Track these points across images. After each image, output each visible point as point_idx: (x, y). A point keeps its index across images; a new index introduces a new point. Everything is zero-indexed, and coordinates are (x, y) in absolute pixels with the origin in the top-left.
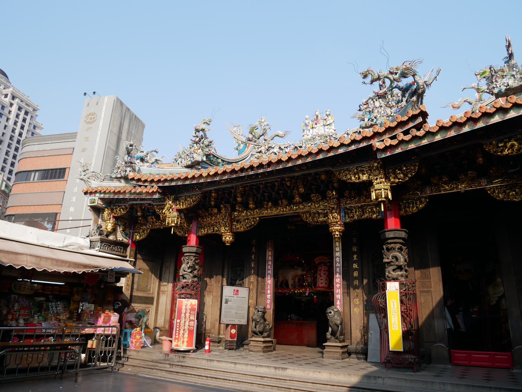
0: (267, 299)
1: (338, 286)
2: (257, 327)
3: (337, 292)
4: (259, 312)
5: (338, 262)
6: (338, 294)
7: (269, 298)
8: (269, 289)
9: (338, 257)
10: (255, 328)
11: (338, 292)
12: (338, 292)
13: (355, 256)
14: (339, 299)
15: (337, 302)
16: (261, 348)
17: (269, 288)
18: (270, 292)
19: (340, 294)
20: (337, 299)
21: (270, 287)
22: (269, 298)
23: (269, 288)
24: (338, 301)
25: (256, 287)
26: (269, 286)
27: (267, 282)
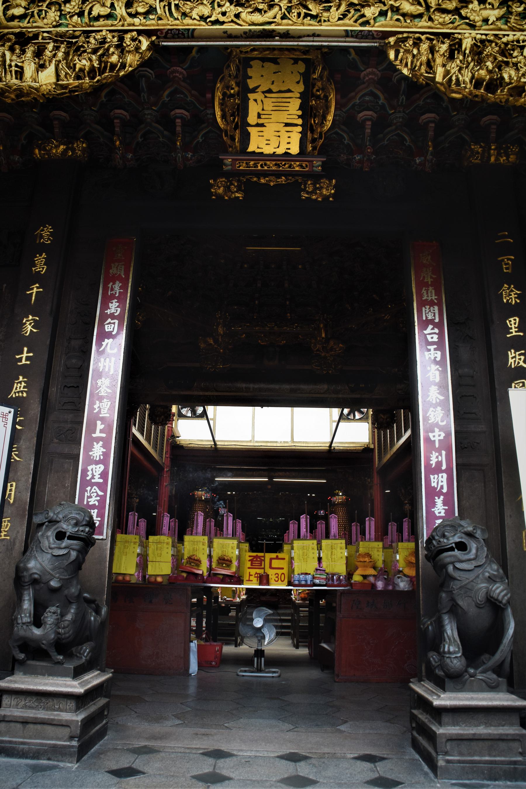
0: (86, 483)
1: (437, 436)
2: (49, 618)
3: (433, 461)
4: (66, 542)
5: (433, 343)
6: (438, 470)
7: (97, 479)
8: (98, 440)
9: (432, 322)
10: (38, 622)
11: (439, 464)
12: (439, 464)
13: (513, 323)
14: (440, 493)
15: (434, 504)
16: (66, 732)
17: (97, 434)
18: (106, 455)
19: (448, 471)
20: (433, 493)
21: (107, 430)
22: (97, 479)
23: (97, 434)
24: (439, 501)
25: (35, 428)
26: (100, 426)
27: (92, 409)
